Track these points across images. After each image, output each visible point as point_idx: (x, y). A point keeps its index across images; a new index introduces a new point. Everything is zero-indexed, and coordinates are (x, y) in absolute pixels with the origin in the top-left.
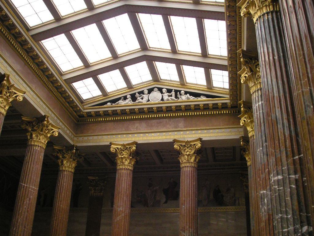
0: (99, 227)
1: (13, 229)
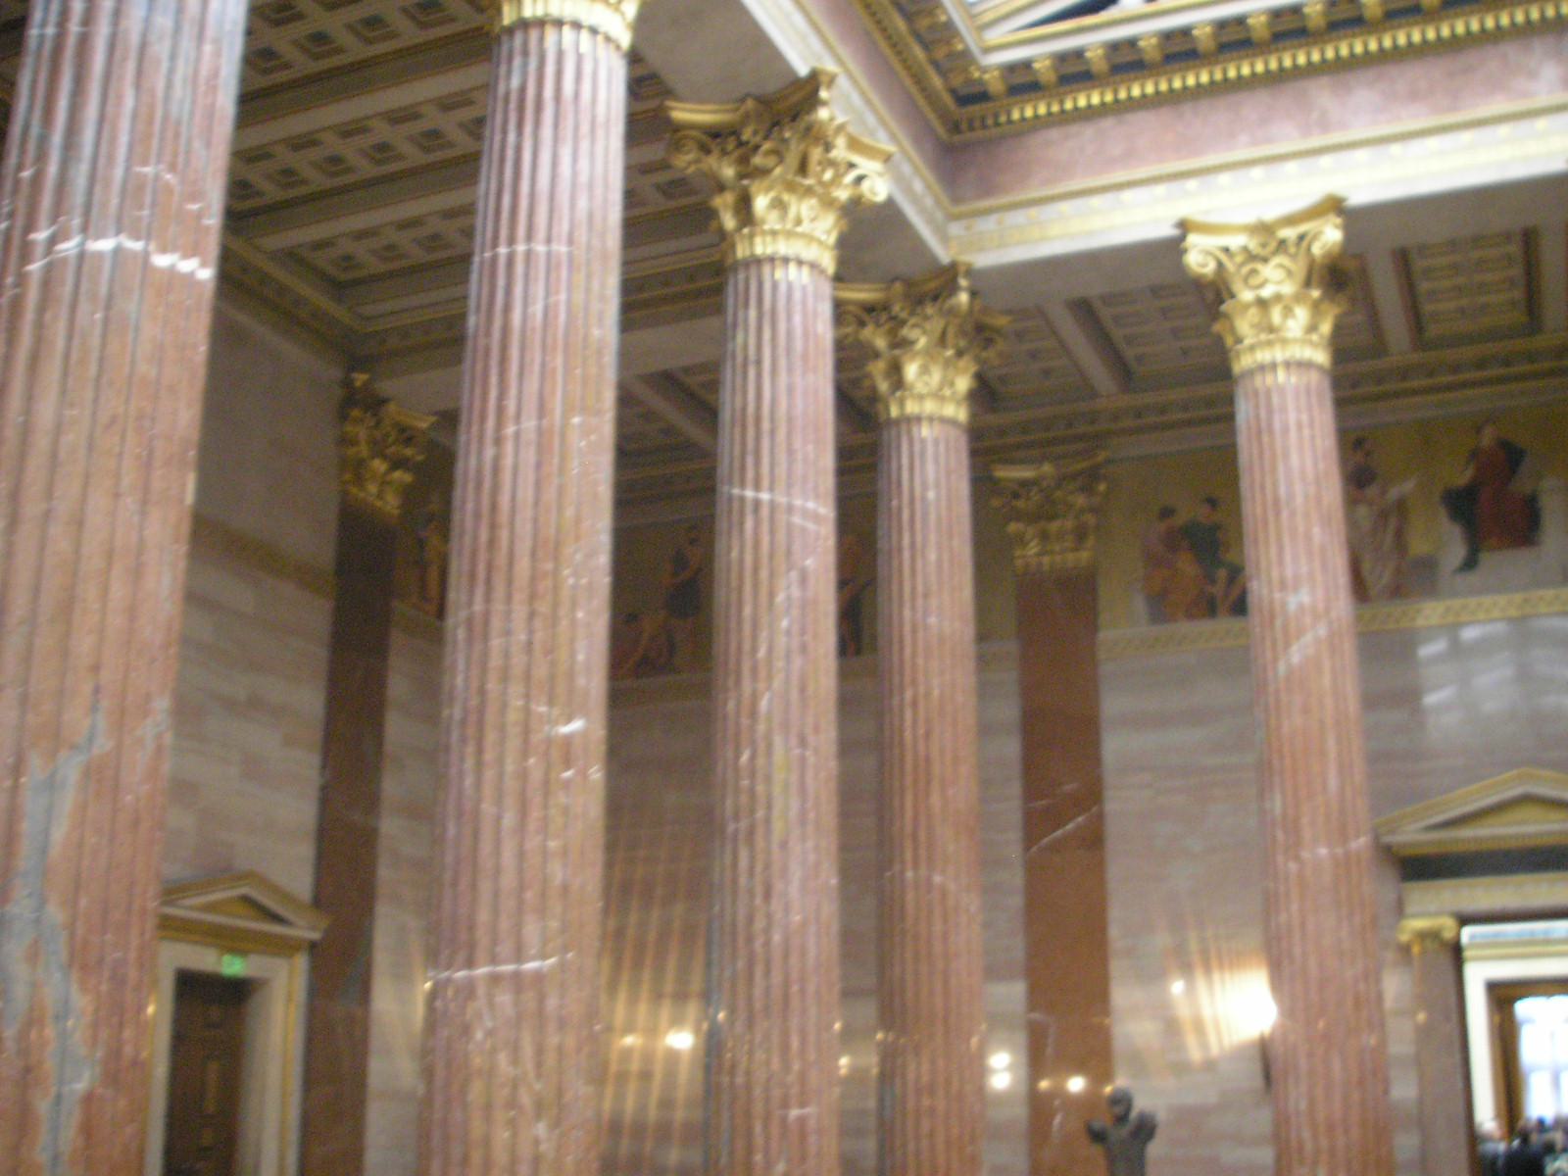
1: (737, 757)
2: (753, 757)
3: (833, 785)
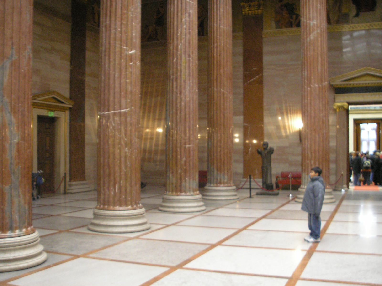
0: (261, 58)
2: (177, 60)
3: (197, 67)
